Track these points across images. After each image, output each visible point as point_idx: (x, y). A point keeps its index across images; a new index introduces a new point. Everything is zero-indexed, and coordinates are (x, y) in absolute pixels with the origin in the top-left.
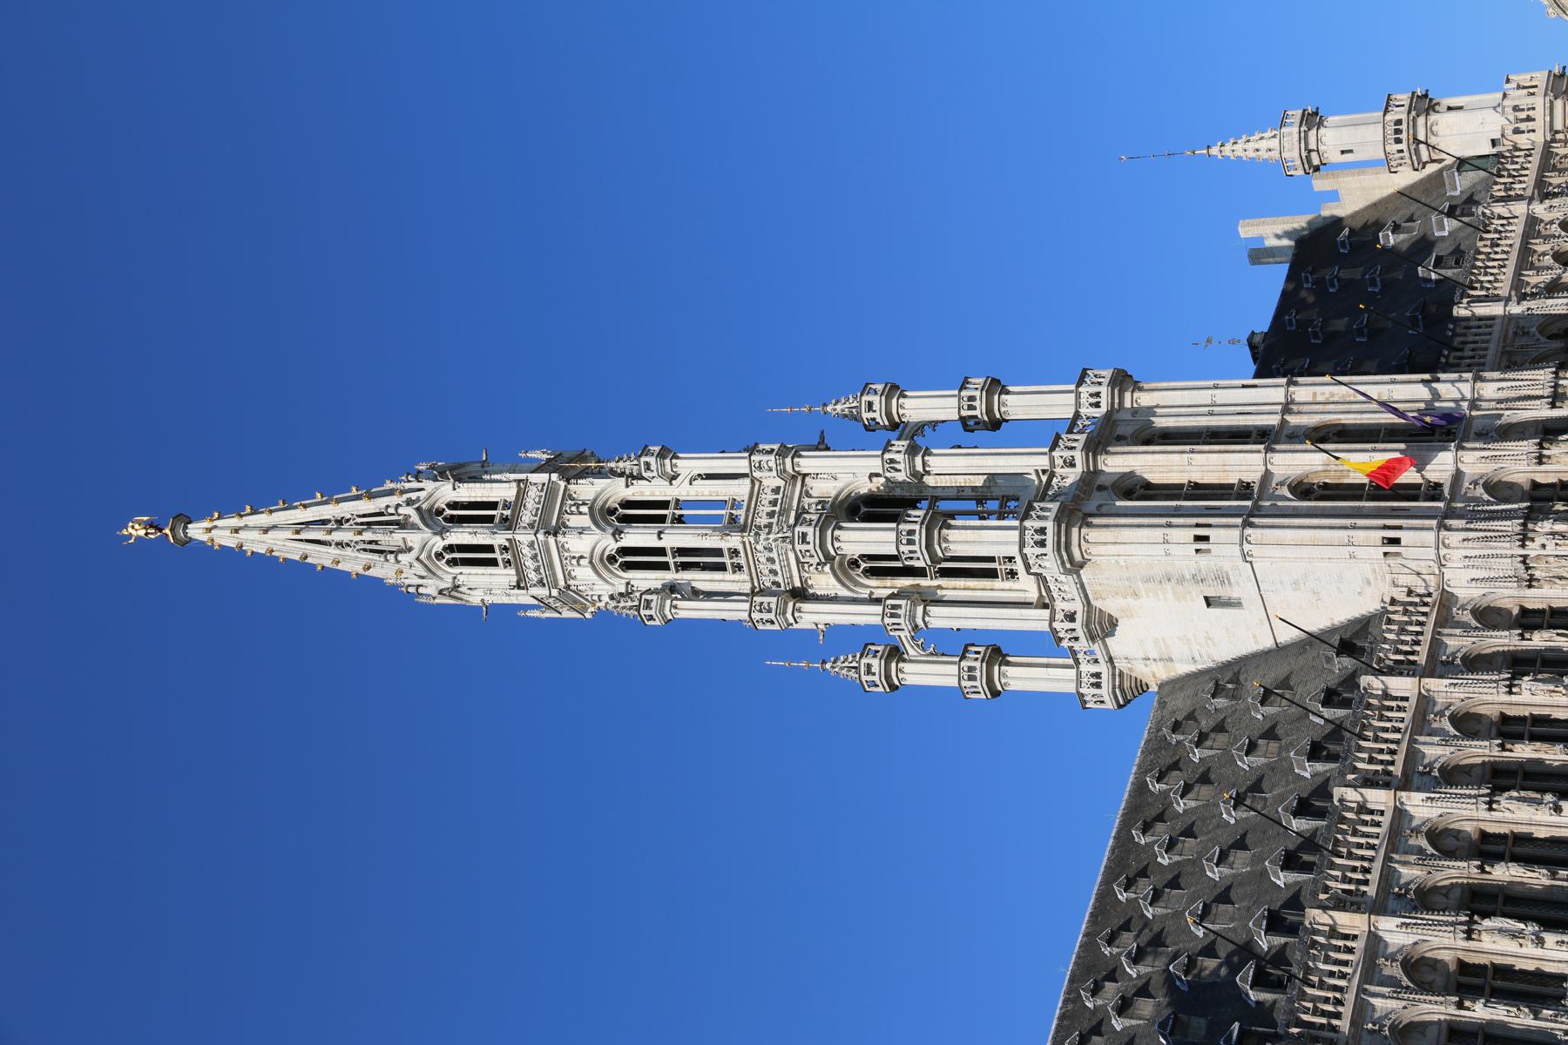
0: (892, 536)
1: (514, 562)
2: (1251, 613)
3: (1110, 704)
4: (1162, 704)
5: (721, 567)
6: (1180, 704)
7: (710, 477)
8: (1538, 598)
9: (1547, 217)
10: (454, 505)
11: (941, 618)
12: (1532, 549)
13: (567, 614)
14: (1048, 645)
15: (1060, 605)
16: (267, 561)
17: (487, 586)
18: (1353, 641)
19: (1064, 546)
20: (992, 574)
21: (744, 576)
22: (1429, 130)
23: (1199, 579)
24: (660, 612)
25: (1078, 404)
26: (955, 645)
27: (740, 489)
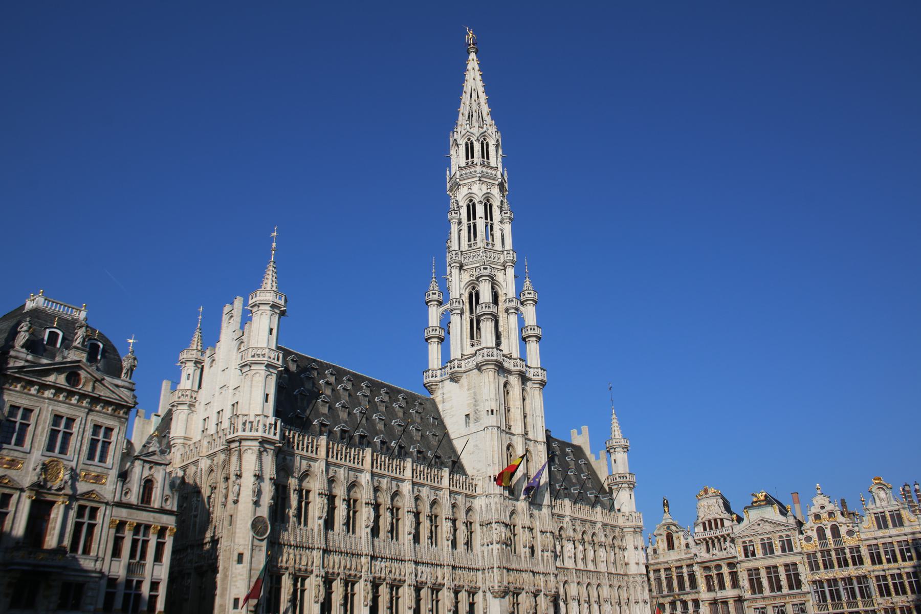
0: (487, 301)
1: (468, 166)
2: (463, 430)
3: (425, 381)
4: (427, 400)
5: (469, 240)
6: (428, 406)
7: (503, 236)
8: (476, 527)
9: (597, 528)
10: (487, 145)
11: (455, 319)
12: (494, 526)
13: (448, 186)
14: (446, 359)
15: (463, 362)
16: (463, 79)
17: (458, 157)
18: (457, 467)
19: (487, 363)
20: (472, 338)
21: (467, 248)
22: (624, 488)
23: (476, 411)
24: (454, 218)
25: (534, 368)
26: (445, 324)
27: (498, 246)
